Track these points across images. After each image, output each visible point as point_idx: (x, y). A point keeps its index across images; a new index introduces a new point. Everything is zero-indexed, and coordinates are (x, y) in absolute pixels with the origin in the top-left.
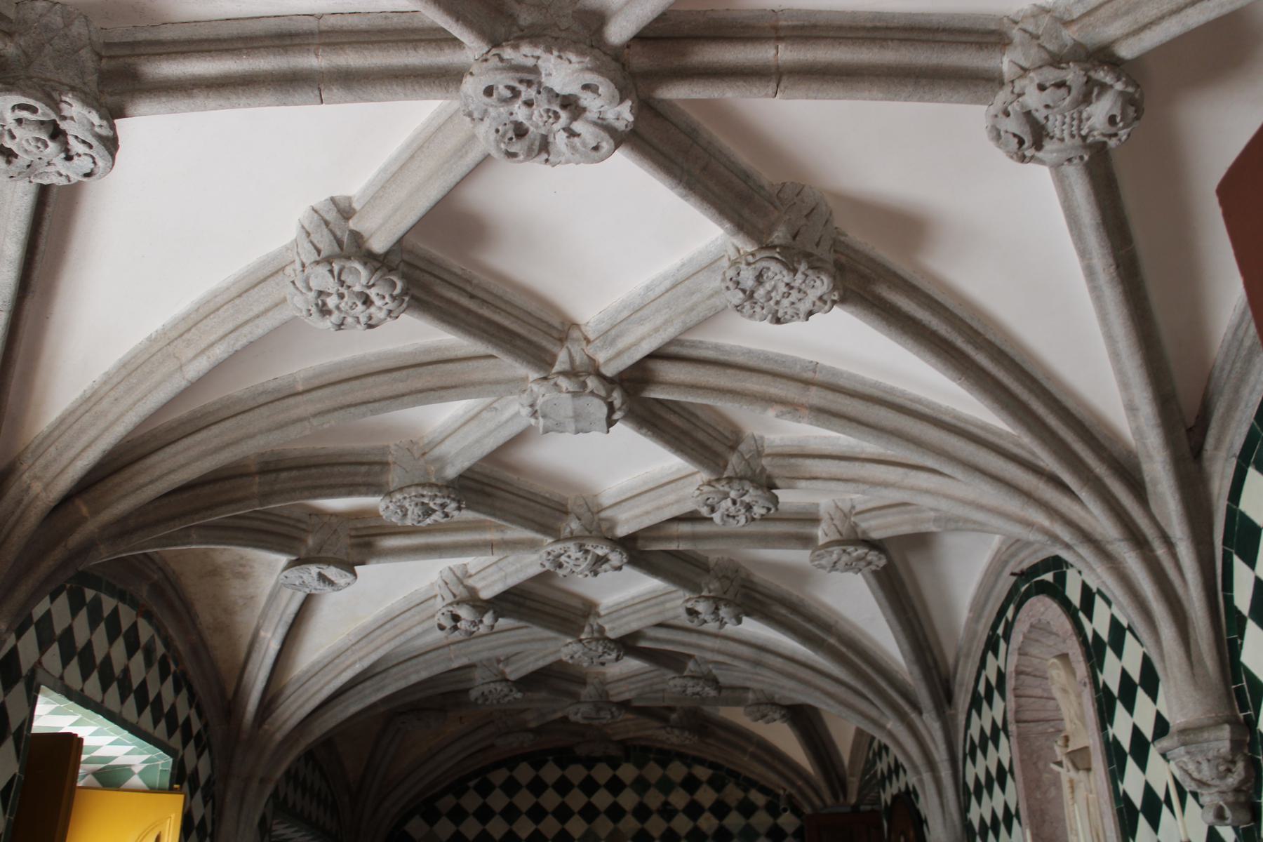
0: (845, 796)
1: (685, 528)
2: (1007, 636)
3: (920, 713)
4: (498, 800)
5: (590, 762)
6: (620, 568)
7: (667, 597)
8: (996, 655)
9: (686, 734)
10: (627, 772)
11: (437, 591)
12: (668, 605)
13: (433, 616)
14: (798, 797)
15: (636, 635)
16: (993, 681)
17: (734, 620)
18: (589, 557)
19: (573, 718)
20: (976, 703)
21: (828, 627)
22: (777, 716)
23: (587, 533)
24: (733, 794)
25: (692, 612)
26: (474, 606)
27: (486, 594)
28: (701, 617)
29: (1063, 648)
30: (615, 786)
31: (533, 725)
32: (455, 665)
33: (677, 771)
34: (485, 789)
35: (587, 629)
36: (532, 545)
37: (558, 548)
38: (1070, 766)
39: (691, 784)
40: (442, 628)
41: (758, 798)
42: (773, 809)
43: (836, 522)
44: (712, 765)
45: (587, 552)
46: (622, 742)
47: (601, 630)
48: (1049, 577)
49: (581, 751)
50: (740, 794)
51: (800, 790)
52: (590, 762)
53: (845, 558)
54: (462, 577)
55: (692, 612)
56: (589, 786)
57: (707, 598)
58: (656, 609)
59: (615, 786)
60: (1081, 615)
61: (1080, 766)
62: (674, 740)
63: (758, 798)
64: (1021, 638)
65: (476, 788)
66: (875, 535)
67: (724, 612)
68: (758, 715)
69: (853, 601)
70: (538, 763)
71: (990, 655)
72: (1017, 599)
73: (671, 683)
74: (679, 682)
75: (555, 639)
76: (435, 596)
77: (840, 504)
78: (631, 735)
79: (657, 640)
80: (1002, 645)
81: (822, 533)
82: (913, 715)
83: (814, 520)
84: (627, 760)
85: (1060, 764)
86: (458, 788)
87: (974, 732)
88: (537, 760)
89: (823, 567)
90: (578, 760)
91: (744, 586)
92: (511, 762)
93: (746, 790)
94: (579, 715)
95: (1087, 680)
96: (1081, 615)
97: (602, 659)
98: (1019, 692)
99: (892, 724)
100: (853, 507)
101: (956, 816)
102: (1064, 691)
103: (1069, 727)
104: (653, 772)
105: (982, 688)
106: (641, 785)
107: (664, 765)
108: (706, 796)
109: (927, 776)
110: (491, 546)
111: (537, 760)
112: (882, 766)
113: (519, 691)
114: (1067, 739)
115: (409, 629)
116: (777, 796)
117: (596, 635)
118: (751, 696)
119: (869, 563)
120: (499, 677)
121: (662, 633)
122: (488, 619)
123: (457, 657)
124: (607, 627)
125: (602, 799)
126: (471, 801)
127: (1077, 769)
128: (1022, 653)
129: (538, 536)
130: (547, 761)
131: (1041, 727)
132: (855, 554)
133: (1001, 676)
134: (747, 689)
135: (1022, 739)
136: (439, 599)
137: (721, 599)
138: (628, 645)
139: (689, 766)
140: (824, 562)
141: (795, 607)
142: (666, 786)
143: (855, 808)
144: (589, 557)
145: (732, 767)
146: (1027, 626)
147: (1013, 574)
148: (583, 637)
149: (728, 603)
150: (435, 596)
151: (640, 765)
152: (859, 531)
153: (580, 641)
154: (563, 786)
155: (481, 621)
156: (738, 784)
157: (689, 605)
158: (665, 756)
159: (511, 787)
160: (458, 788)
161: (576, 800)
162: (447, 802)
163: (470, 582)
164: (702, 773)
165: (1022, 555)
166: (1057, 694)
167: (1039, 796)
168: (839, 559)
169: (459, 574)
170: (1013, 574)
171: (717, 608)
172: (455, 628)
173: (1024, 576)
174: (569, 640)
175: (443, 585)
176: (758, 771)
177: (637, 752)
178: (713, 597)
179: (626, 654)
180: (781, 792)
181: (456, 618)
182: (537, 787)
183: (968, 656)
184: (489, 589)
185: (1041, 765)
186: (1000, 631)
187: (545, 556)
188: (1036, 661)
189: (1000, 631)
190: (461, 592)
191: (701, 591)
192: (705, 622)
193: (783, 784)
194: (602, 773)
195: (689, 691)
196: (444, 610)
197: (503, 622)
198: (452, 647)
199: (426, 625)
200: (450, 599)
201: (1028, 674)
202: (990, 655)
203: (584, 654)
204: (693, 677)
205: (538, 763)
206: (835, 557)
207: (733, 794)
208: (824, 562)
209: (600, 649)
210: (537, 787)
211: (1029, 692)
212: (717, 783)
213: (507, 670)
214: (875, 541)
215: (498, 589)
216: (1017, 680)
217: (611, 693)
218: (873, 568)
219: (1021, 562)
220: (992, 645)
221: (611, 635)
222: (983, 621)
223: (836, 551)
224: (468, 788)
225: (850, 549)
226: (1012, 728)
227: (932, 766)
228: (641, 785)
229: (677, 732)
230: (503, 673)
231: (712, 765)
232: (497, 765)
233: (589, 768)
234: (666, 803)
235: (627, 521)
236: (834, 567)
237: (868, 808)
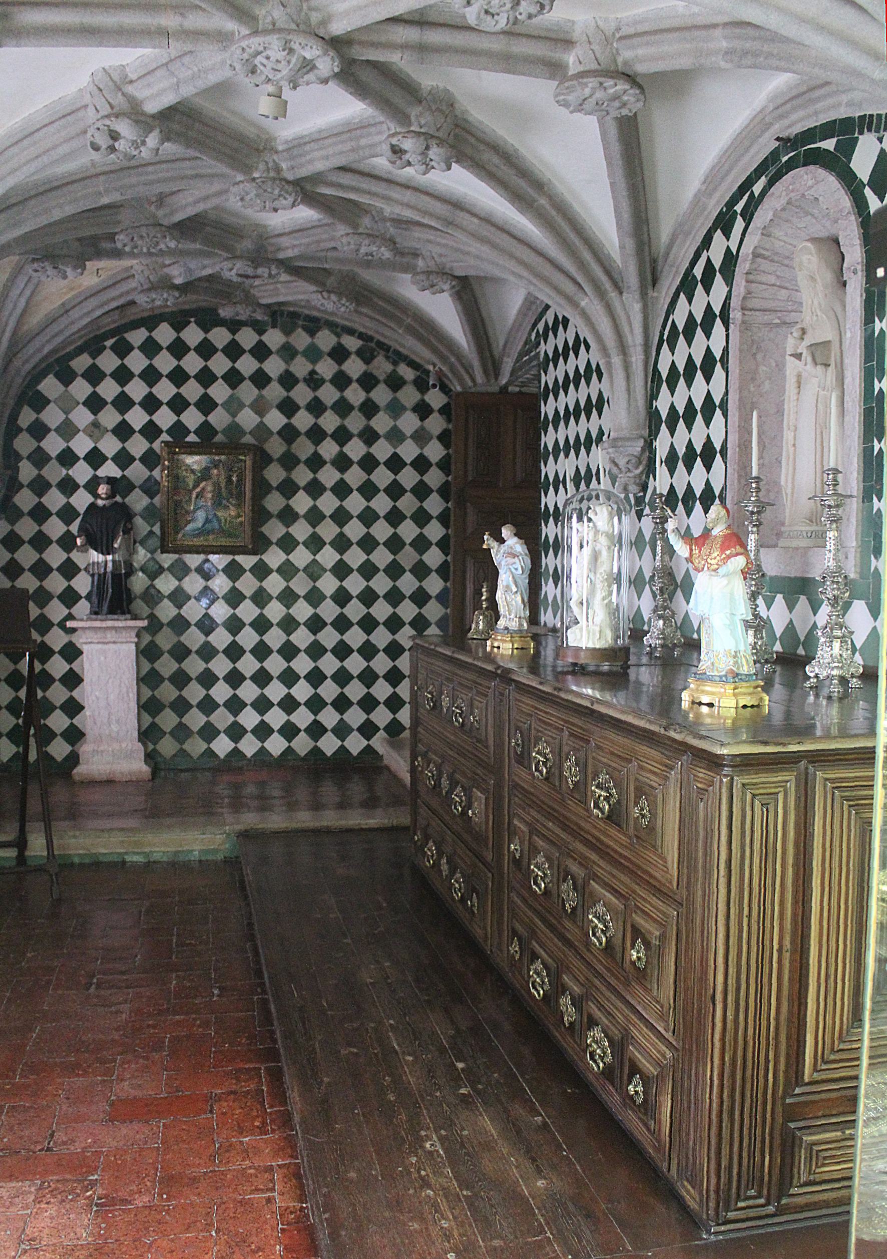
0: (496, 379)
1: (411, 34)
2: (748, 215)
3: (621, 293)
4: (137, 362)
5: (234, 326)
6: (325, 81)
7: (365, 131)
8: (727, 236)
9: (344, 301)
10: (274, 338)
11: (87, 99)
12: (363, 142)
13: (85, 132)
14: (450, 375)
15: (317, 178)
16: (717, 264)
17: (443, 165)
18: (294, 60)
19: (227, 275)
20: (687, 286)
21: (539, 185)
22: (446, 287)
23: (294, 27)
24: (382, 366)
25: (397, 151)
26: (137, 122)
27: (152, 107)
28: (406, 157)
29: (823, 230)
30: (261, 352)
31: (178, 281)
32: (105, 200)
33: (325, 340)
34: (123, 349)
35: (262, 166)
36: (223, 38)
37: (255, 43)
38: (809, 359)
39: (339, 354)
40: (96, 148)
41: (407, 373)
42: (421, 385)
43: (595, 47)
44: (361, 336)
45: (291, 51)
46: (268, 306)
47: (278, 170)
48: (829, 144)
49: (225, 312)
50: (389, 367)
51: (452, 368)
52: (234, 326)
53: (599, 95)
54: (118, 82)
55: (397, 151)
56: (233, 351)
57: (419, 134)
58: (348, 146)
59: (261, 352)
60: (868, 191)
61: (818, 360)
62: (330, 307)
63: (407, 373)
64: (770, 215)
65: (112, 348)
66: (641, 68)
67: (435, 153)
68: (426, 284)
69: (575, 156)
70: (179, 326)
71: (718, 235)
72: (772, 170)
73: (344, 240)
74: (353, 240)
75: (222, 176)
76: (86, 106)
77: (600, 23)
78: (281, 299)
79: (340, 186)
80: (739, 224)
81: (572, 60)
82: (613, 295)
83: (568, 43)
84: (274, 326)
85: (798, 356)
86: (94, 346)
87: (680, 318)
88: (179, 322)
89: (566, 104)
90: (222, 323)
91: (457, 126)
92: (151, 322)
93: (395, 363)
94: (234, 271)
95: (859, 267)
96: (868, 191)
97: (276, 204)
98: (751, 277)
99: (590, 303)
100: (618, 29)
101: (641, 402)
102: (812, 279)
103: (807, 318)
104: (301, 340)
105: (698, 271)
106: (288, 352)
107: (312, 333)
108: (354, 367)
109: (617, 360)
110: (165, 33)
111: (179, 322)
112: (547, 348)
113: (173, 238)
114: (804, 331)
115: (55, 147)
116: (427, 372)
117: (272, 174)
118: (420, 263)
119: (624, 105)
120: (151, 221)
121: (346, 179)
122: (152, 140)
123: (107, 191)
124: (284, 166)
125: (247, 365)
126: (108, 362)
127: (815, 363)
128: (766, 233)
129: (231, 25)
130: (190, 322)
131: (767, 317)
132: (612, 91)
133: (730, 259)
134: (416, 255)
135: (746, 326)
136: (91, 111)
137: (432, 137)
138: (305, 190)
139: (338, 336)
140: (570, 98)
141: (508, 157)
142: (313, 354)
143: (504, 390)
144: (294, 60)
145: (382, 339)
146: (783, 201)
147: (778, 139)
148: (256, 175)
149: (441, 142)
150: (86, 106)
151: (287, 332)
152: (620, 60)
153: (254, 179)
154: (206, 350)
155: (144, 143)
156: (387, 358)
157: (394, 141)
158: (313, 325)
159: (150, 348)
160: (93, 345)
161: (220, 364)
162: (82, 363)
163: (130, 89)
164: (351, 343)
165: (794, 117)
166: (803, 282)
167: (752, 389)
168: (591, 96)
169: (116, 77)
170: (778, 139)
171: (427, 148)
172: (112, 149)
173: (786, 143)
174: (240, 177)
175: (96, 91)
176: (411, 345)
177: (283, 316)
178: (424, 134)
179: (302, 202)
180: (431, 368)
181: (114, 136)
182: (178, 349)
183: (688, 234)
184: (157, 97)
185: (759, 357)
186: (739, 208)
187: (239, 51)
188: (778, 244)
189: (739, 208)
190: (118, 100)
191: (410, 124)
192: (409, 164)
193: (436, 361)
194: (247, 338)
195: (363, 250)
196: (99, 124)
197: (170, 148)
198: (102, 178)
199: (75, 144)
200: (107, 110)
201: (765, 258)
202: (718, 235)
203: (257, 195)
204: (369, 235)
205: (179, 326)
206: (587, 91)
207: (382, 366)
208: (570, 98)
209: (276, 192)
210: (178, 349)
211: (763, 278)
212: (367, 356)
213: (160, 213)
214: (636, 74)
215: (169, 99)
216: (753, 262)
217: (270, 249)
218: (625, 112)
219: (789, 126)
220: (724, 223)
221: (290, 177)
222: (717, 195)
223: (592, 82)
224: (105, 348)
225: (609, 83)
226: (735, 315)
227: (623, 349)
228: (288, 352)
229: (334, 297)
230: (154, 216)
231: (361, 336)
232: (135, 325)
233: (234, 332)
234: (313, 372)
235: (347, 13)
236: (580, 108)
237: (517, 389)
